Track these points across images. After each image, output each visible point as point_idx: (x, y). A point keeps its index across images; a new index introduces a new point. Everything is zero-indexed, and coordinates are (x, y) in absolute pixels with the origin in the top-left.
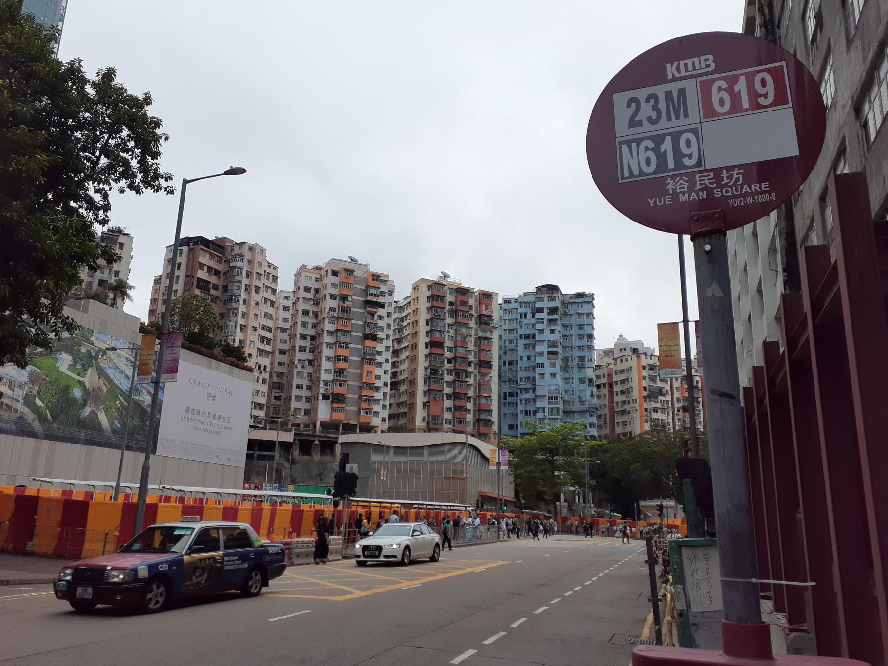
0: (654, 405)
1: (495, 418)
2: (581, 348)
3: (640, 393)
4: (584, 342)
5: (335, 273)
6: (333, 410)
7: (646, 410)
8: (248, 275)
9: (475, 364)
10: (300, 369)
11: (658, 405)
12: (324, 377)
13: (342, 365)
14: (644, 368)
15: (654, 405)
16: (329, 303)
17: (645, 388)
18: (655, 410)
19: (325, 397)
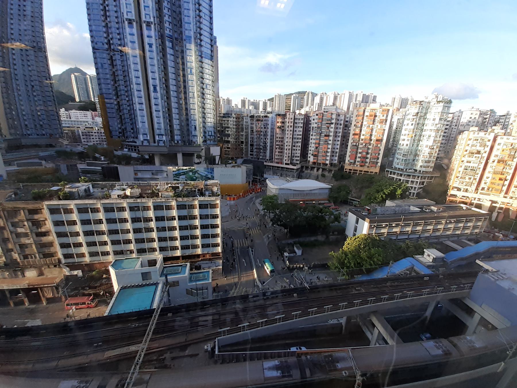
1: (380, 161)
8: (289, 122)
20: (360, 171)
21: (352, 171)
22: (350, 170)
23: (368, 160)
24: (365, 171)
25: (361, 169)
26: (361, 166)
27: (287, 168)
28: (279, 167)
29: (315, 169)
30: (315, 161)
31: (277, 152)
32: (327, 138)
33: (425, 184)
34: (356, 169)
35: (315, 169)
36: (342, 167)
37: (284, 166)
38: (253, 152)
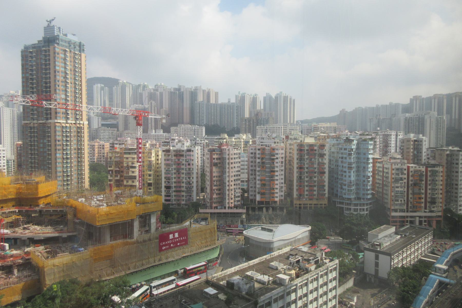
0: (396, 185)
2: (364, 163)
3: (391, 180)
4: (365, 161)
5: (259, 150)
6: (261, 198)
7: (393, 187)
9: (318, 172)
10: (251, 181)
11: (399, 185)
12: (258, 186)
13: (263, 182)
14: (393, 170)
15: (396, 185)
16: (258, 160)
17: (393, 178)
18: (397, 187)
19: (259, 193)
20: (310, 204)
21: (302, 206)
22: (300, 204)
23: (315, 193)
24: (315, 204)
25: (310, 202)
26: (311, 199)
27: (231, 213)
28: (220, 213)
29: (264, 209)
30: (263, 200)
31: (215, 194)
32: (272, 173)
33: (369, 209)
34: (306, 202)
35: (264, 209)
36: (292, 202)
37: (227, 211)
38: (169, 196)
